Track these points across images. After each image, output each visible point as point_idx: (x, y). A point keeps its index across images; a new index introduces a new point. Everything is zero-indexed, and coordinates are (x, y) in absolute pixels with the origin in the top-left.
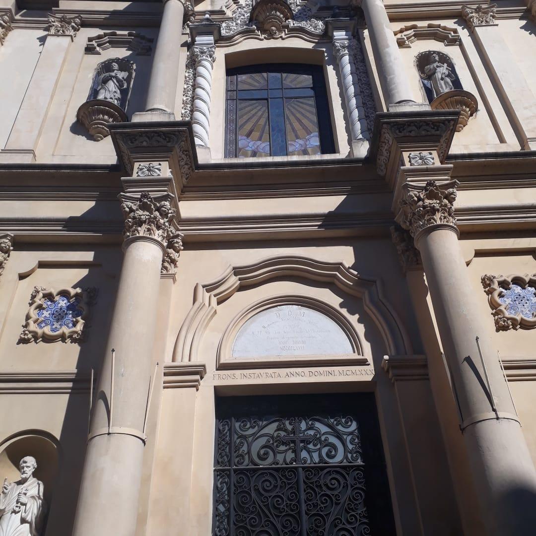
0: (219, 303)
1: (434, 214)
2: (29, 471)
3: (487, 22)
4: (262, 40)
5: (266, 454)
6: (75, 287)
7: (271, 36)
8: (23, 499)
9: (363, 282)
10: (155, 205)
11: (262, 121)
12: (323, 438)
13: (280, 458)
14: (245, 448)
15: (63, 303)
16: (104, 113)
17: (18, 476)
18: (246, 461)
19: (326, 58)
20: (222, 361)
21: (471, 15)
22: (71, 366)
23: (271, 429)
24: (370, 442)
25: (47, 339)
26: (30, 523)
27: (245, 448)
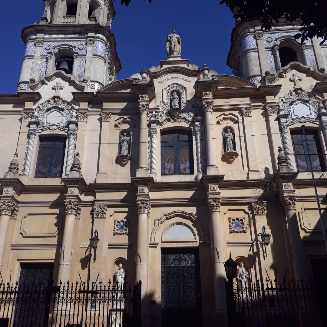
0: (161, 224)
2: (121, 267)
5: (173, 262)
6: (124, 219)
7: (175, 121)
8: (121, 273)
9: (197, 219)
10: (145, 203)
11: (172, 155)
12: (186, 259)
13: (176, 263)
14: (168, 261)
15: (122, 224)
16: (125, 158)
17: (118, 268)
18: (168, 264)
20: (162, 241)
22: (126, 242)
23: (174, 256)
26: (123, 278)
27: (168, 261)
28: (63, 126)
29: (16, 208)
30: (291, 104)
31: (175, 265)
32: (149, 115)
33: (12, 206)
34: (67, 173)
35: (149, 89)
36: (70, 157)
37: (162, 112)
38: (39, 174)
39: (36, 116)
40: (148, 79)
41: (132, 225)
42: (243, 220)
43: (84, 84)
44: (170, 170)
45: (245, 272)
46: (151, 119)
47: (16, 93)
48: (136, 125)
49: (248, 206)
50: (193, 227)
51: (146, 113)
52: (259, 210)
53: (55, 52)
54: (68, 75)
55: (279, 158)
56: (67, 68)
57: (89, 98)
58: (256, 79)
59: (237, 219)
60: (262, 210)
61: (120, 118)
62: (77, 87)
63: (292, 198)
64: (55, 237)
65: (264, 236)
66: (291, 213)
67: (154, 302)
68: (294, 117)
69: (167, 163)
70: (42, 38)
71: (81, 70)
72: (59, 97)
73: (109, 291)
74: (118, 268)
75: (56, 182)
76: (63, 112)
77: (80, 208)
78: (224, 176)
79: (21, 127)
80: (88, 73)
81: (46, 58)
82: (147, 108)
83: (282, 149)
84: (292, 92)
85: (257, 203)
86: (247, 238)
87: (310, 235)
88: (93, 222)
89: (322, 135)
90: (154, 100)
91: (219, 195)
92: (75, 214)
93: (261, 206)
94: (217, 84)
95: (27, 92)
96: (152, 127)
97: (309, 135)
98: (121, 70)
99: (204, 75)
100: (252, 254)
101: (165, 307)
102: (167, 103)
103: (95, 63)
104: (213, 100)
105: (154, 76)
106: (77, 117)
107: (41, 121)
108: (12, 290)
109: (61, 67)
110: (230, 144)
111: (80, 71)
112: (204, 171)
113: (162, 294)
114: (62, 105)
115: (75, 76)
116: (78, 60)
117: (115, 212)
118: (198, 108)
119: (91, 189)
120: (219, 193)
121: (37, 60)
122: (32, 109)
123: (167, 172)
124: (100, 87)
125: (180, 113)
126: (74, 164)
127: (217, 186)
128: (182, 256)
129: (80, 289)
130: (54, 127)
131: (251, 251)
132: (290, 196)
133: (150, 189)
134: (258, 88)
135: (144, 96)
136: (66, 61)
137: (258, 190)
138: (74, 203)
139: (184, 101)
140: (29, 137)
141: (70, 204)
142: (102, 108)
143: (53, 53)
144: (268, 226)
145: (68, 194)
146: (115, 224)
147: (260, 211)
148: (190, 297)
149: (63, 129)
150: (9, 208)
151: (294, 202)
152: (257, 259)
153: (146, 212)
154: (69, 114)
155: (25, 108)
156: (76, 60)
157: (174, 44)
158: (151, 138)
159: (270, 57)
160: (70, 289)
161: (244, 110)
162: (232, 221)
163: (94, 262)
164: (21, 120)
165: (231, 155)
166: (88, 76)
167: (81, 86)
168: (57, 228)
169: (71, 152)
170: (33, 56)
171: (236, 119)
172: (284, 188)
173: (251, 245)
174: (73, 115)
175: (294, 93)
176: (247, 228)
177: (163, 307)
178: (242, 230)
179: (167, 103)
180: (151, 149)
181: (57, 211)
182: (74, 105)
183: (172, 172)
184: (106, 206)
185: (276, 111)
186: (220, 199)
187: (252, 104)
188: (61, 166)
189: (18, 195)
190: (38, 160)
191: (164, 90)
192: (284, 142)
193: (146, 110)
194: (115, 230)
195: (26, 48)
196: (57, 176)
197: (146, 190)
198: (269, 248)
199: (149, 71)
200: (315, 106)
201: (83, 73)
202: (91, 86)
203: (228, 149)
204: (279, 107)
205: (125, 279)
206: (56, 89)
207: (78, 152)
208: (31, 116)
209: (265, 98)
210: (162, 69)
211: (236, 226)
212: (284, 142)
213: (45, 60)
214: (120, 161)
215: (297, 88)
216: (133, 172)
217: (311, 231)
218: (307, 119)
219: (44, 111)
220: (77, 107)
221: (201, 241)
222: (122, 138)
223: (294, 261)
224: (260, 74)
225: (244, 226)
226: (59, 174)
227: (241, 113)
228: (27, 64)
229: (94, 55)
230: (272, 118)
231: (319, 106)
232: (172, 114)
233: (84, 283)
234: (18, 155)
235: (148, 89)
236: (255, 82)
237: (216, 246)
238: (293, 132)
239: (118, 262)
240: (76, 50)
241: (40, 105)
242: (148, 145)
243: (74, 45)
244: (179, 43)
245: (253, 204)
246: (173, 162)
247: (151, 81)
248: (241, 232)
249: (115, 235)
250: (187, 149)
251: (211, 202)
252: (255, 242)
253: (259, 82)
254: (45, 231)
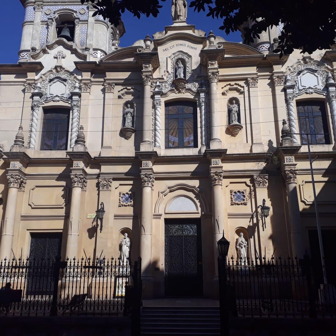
0: (164, 196)
1: (216, 181)
2: (126, 236)
4: (176, 94)
6: (129, 191)
7: (180, 92)
8: (126, 242)
9: (200, 192)
13: (179, 233)
14: (171, 231)
15: (127, 196)
16: (129, 131)
17: (124, 237)
19: (197, 104)
20: (166, 212)
21: (250, 81)
23: (177, 227)
24: (199, 230)
25: (125, 206)
27: (171, 231)
28: (66, 98)
29: (24, 181)
30: (299, 74)
31: (178, 234)
32: (152, 85)
33: (20, 179)
34: (72, 146)
35: (153, 58)
36: (74, 130)
38: (44, 146)
39: (39, 87)
40: (152, 46)
41: (136, 197)
42: (245, 192)
43: (86, 53)
44: (174, 142)
45: (244, 242)
46: (155, 90)
47: (18, 63)
48: (139, 96)
49: (250, 179)
50: (195, 199)
51: (149, 84)
52: (260, 183)
53: (56, 18)
54: (70, 43)
55: (283, 131)
56: (69, 35)
57: (92, 68)
58: (264, 47)
59: (239, 192)
60: (264, 183)
61: (124, 89)
62: (79, 55)
63: (294, 172)
64: (63, 208)
65: (264, 208)
66: (292, 186)
67: (158, 269)
68: (301, 88)
69: (171, 136)
70: (42, 2)
71: (83, 37)
72: (61, 67)
73: (112, 266)
74: (124, 237)
75: (61, 154)
76: (66, 83)
77: (86, 180)
78: (226, 150)
79: (24, 98)
80: (90, 40)
81: (46, 25)
82: (151, 79)
83: (286, 122)
84: (300, 60)
85: (259, 176)
86: (247, 209)
87: (310, 208)
88: (99, 194)
89: (328, 106)
90: (158, 69)
91: (221, 169)
92: (82, 187)
93: (262, 179)
94: (223, 54)
95: (28, 61)
96: (156, 99)
97: (316, 106)
98: (125, 34)
99: (210, 42)
100: (252, 225)
101: (168, 273)
102: (172, 73)
103: (97, 29)
104: (219, 70)
105: (158, 43)
106: (80, 88)
107: (44, 93)
108: (23, 265)
109: (63, 34)
110: (235, 116)
111: (82, 38)
112: (208, 145)
113: (165, 262)
114: (64, 75)
115: (77, 44)
116: (79, 26)
117: (120, 185)
118: (203, 78)
119: (97, 162)
120: (222, 167)
121: (37, 26)
122: (35, 79)
123: (171, 145)
124: (103, 55)
125: (185, 83)
126: (78, 137)
127: (220, 160)
128: (184, 226)
129: (85, 265)
130: (57, 99)
131: (251, 222)
132: (292, 170)
133: (154, 163)
134: (265, 56)
135: (148, 65)
136: (68, 27)
137: (261, 163)
138: (79, 177)
139: (189, 70)
140: (33, 109)
141: (76, 177)
142: (105, 78)
143: (54, 18)
144: (269, 198)
145: (74, 168)
146: (120, 196)
147: (261, 184)
148: (191, 264)
149: (67, 101)
150: (17, 181)
151: (294, 176)
152: (256, 229)
153: (150, 185)
154: (72, 85)
155: (27, 78)
156: (77, 26)
157: (180, 8)
158: (155, 110)
160: (76, 264)
161: (250, 80)
162: (233, 194)
163: (101, 232)
164: (24, 91)
165: (235, 128)
166: (91, 44)
167: (83, 54)
168: (64, 199)
169: (75, 124)
170: (33, 22)
171: (242, 89)
172: (286, 161)
173: (251, 216)
174: (76, 86)
175: (302, 62)
176: (247, 199)
177: (166, 273)
178: (243, 202)
179: (172, 73)
180: (155, 121)
181: (63, 183)
182: (76, 75)
183: (176, 145)
184: (111, 179)
185: (283, 81)
186: (222, 172)
187: (259, 74)
188: (65, 138)
189: (25, 167)
190: (43, 132)
191: (168, 58)
192: (289, 114)
193: (150, 81)
194: (121, 201)
195: (24, 17)
196: (63, 148)
197: (150, 164)
198: (268, 220)
199: (153, 37)
200: (324, 76)
201: (85, 40)
202: (94, 55)
203: (232, 122)
204: (286, 77)
205: (131, 247)
206: (58, 58)
207: (82, 125)
208: (34, 87)
209: (272, 67)
210: (166, 35)
211: (237, 198)
212: (289, 114)
213: (45, 26)
214: (124, 133)
215: (306, 57)
216: (137, 147)
217: (311, 203)
218: (314, 90)
219: (47, 82)
220: (79, 77)
221: (203, 213)
222: (125, 109)
223: (292, 232)
224: (268, 41)
225: (245, 199)
226: (64, 146)
227: (247, 83)
228: (27, 30)
229: (95, 21)
230: (279, 89)
231: (327, 75)
232: (176, 84)
233: (89, 259)
234: (22, 128)
235: (152, 58)
236: (263, 50)
237: (216, 218)
238: (299, 103)
239: (124, 231)
240: (78, 15)
241: (42, 76)
242: (152, 117)
243: (75, 10)
244: (185, 7)
245: (255, 177)
246: (177, 135)
247: (156, 49)
248: (242, 204)
249: (120, 206)
250: (191, 121)
251: (213, 176)
252: (255, 214)
253: (267, 50)
254: (53, 203)
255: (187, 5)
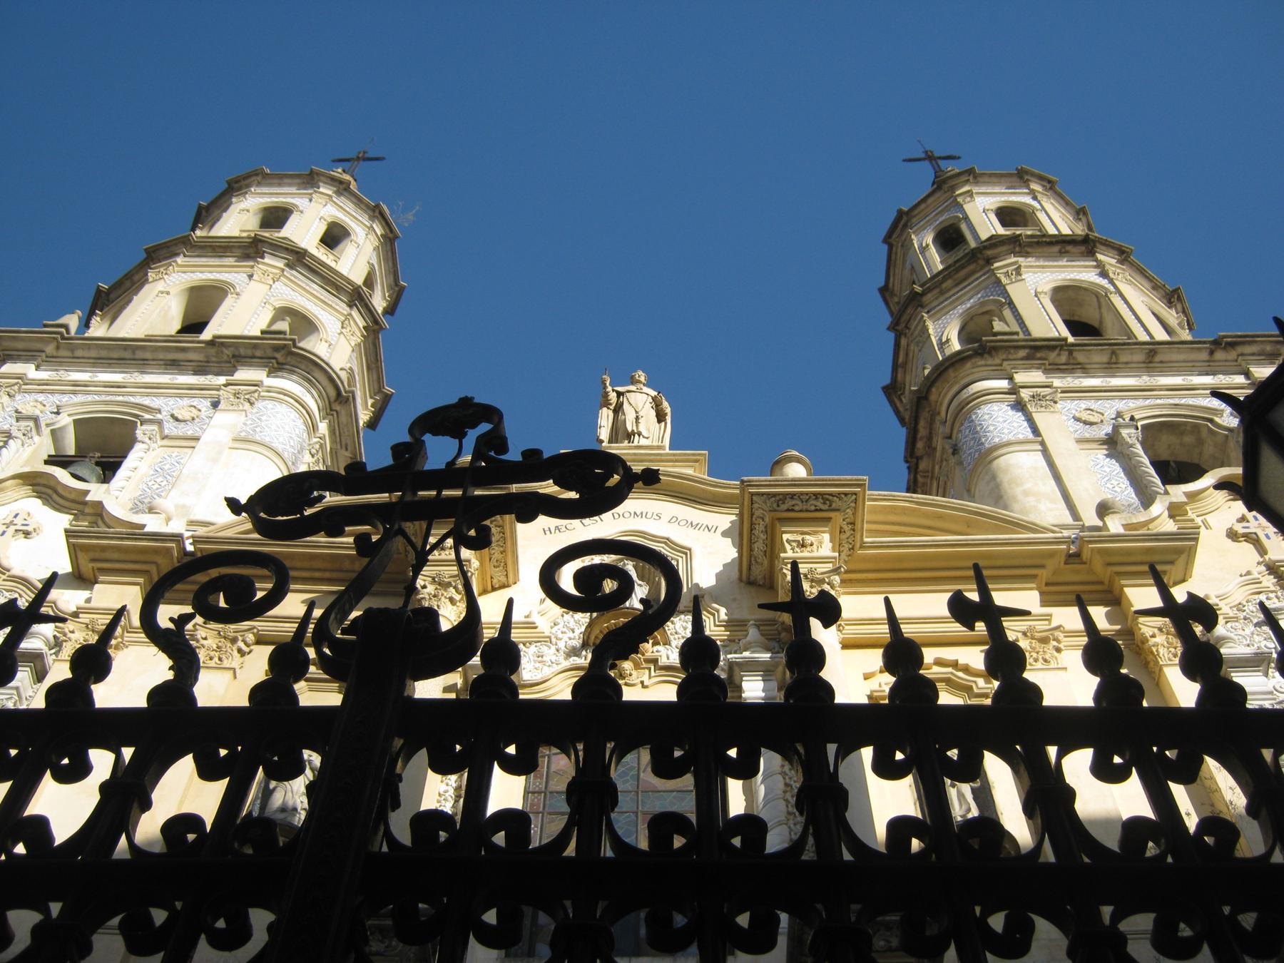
3: (1045, 661)
37: (548, 640)
143: (48, 425)
159: (1108, 470)
255: (668, 410)
